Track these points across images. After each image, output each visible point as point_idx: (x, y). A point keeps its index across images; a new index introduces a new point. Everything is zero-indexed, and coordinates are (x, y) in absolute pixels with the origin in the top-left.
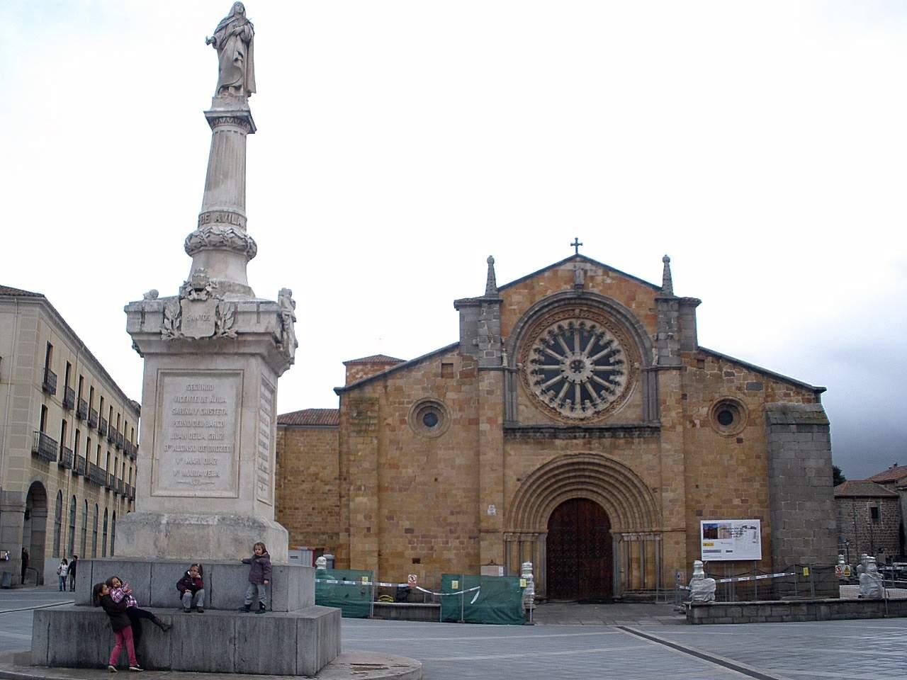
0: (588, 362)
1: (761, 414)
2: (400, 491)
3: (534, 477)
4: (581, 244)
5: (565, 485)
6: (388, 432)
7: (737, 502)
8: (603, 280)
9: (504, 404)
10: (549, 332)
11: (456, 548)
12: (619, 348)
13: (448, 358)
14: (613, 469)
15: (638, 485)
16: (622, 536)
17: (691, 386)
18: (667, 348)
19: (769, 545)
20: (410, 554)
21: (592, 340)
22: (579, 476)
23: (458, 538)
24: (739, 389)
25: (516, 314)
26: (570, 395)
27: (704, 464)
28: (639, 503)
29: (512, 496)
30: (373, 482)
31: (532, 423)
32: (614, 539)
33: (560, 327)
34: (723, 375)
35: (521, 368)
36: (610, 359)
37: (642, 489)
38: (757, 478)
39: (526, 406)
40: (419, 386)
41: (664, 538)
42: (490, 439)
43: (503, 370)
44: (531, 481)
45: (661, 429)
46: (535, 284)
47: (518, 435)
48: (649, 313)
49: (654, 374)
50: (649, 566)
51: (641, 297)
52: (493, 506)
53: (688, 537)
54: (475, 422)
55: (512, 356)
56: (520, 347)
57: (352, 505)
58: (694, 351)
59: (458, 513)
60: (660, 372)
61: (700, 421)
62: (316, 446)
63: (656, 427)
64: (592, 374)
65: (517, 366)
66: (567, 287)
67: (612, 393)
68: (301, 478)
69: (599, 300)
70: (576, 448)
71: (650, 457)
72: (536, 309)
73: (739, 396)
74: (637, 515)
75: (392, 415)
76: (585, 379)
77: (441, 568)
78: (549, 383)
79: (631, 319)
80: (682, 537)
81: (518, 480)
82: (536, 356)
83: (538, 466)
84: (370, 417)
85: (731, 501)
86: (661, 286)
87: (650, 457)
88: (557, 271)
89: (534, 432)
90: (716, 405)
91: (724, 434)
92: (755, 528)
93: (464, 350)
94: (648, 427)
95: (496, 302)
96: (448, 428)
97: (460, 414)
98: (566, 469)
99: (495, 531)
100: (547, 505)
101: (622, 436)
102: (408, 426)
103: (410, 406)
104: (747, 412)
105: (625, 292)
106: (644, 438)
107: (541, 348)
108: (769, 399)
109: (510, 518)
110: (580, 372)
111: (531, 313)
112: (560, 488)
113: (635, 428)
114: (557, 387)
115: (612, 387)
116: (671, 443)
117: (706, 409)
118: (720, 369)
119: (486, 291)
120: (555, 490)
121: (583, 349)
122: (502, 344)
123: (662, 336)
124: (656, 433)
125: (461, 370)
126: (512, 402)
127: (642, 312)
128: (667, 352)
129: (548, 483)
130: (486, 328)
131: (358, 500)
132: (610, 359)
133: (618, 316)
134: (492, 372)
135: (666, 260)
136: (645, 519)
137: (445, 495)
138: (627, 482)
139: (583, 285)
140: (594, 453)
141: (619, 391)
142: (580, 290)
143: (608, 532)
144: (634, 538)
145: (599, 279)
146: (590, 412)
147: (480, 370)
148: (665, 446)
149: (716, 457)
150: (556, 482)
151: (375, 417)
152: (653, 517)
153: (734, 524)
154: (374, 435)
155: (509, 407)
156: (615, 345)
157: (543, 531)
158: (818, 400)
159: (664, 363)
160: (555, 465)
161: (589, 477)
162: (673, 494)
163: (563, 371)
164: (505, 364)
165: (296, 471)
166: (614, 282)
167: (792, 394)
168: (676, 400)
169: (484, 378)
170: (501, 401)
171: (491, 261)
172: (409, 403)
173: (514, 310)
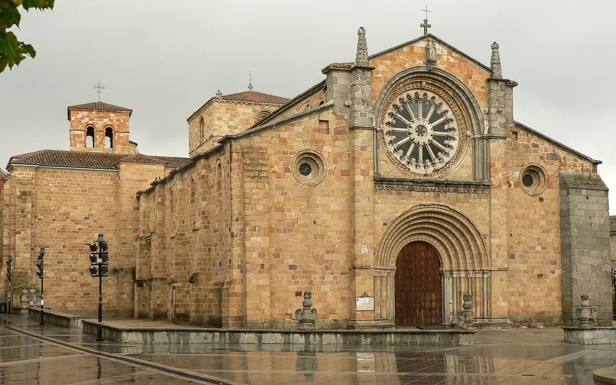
0: (429, 127)
4: (430, 27)
7: (538, 248)
10: (400, 99)
11: (330, 282)
12: (453, 117)
15: (473, 232)
23: (332, 273)
24: (542, 158)
26: (415, 154)
27: (517, 217)
29: (380, 238)
33: (408, 96)
34: (531, 146)
37: (475, 235)
39: (386, 162)
43: (373, 129)
49: (485, 141)
58: (510, 125)
59: (333, 252)
62: (66, 187)
66: (420, 62)
67: (447, 154)
68: (51, 217)
69: (445, 75)
71: (482, 209)
73: (542, 163)
75: (277, 164)
76: (427, 142)
77: (318, 300)
78: (399, 143)
81: (385, 224)
82: (390, 120)
85: (534, 248)
87: (482, 209)
97: (334, 165)
98: (418, 216)
103: (293, 156)
111: (393, 82)
115: (447, 150)
116: (498, 197)
117: (518, 173)
121: (425, 116)
123: (493, 110)
124: (486, 190)
130: (360, 91)
131: (254, 239)
133: (457, 91)
134: (365, 132)
135: (495, 47)
137: (322, 236)
138: (462, 229)
140: (441, 204)
141: (452, 153)
142: (432, 66)
145: (445, 58)
146: (430, 170)
148: (494, 201)
156: (450, 115)
158: (595, 171)
159: (494, 133)
165: (46, 210)
166: (456, 62)
169: (359, 135)
170: (372, 157)
171: (362, 33)
172: (292, 153)
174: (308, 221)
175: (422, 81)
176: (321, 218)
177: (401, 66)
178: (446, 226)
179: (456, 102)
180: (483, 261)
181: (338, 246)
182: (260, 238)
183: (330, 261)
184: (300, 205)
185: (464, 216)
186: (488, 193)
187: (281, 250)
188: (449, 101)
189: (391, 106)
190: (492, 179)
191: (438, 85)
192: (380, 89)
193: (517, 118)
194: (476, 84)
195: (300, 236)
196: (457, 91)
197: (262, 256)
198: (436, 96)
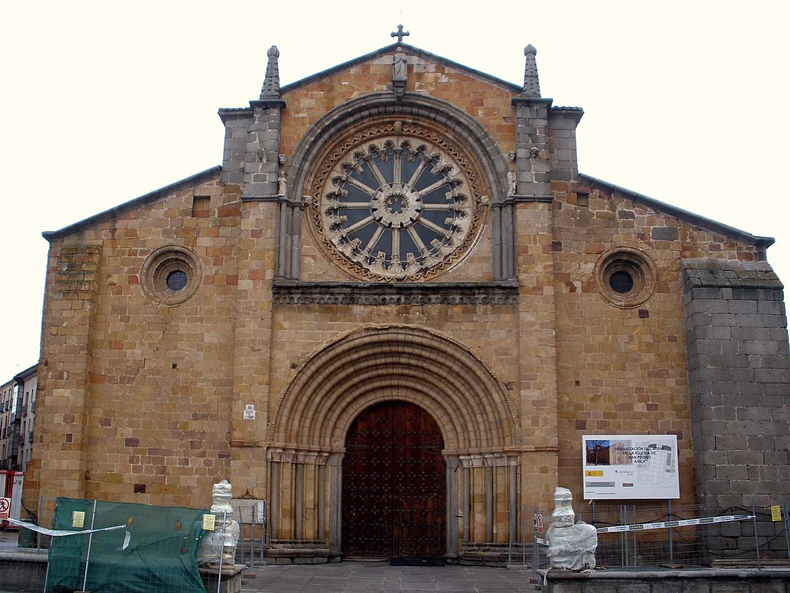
0: (412, 198)
1: (675, 274)
2: (122, 381)
3: (319, 363)
4: (408, 34)
5: (371, 379)
6: (111, 296)
8: (436, 79)
9: (278, 251)
10: (357, 155)
12: (461, 177)
13: (204, 189)
14: (445, 352)
15: (483, 377)
16: (460, 460)
17: (568, 230)
18: (530, 170)
19: (692, 475)
20: (132, 477)
21: (421, 167)
22: (393, 365)
23: (203, 455)
24: (642, 236)
27: (589, 349)
28: (484, 407)
29: (283, 391)
30: (79, 368)
31: (318, 280)
32: (448, 465)
33: (373, 149)
37: (489, 385)
38: (671, 371)
39: (314, 257)
40: (159, 229)
41: (523, 462)
42: (253, 303)
43: (279, 201)
44: (313, 368)
45: (520, 291)
46: (336, 84)
47: (296, 297)
48: (504, 123)
49: (509, 209)
50: (499, 506)
51: (490, 102)
52: (253, 406)
53: (561, 463)
54: (233, 280)
55: (296, 182)
56: (309, 173)
57: (48, 400)
58: (572, 181)
59: (205, 417)
60: (518, 206)
61: (582, 282)
63: (511, 288)
65: (303, 199)
66: (383, 88)
67: (449, 242)
69: (429, 105)
70: (386, 317)
71: (502, 333)
72: (335, 118)
73: (642, 247)
74: (482, 427)
75: (118, 271)
76: (406, 221)
79: (476, 131)
80: (552, 461)
81: (294, 366)
82: (335, 189)
83: (325, 345)
84: (85, 273)
85: (629, 407)
86: (522, 85)
87: (502, 333)
88: (369, 66)
90: (605, 261)
91: (619, 303)
92: (669, 448)
93: (227, 178)
94: (499, 287)
95: (274, 105)
96: (197, 289)
97: (214, 269)
98: (370, 351)
99: (253, 445)
100: (344, 410)
101: (457, 301)
102: (139, 286)
103: (145, 257)
104: (654, 272)
105: (469, 94)
106: (493, 305)
107: (344, 177)
108: (688, 253)
109: (277, 424)
110: (400, 212)
111: (327, 123)
112: (363, 382)
113: (479, 288)
114: (365, 234)
115: (448, 234)
116: (534, 312)
117: (591, 266)
118: (613, 208)
120: (355, 386)
121: (405, 180)
122: (280, 165)
123: (522, 153)
125: (221, 204)
127: (493, 122)
128: (529, 176)
129: (342, 375)
130: (257, 141)
134: (262, 206)
135: (530, 52)
136: (494, 432)
137: (186, 390)
139: (405, 82)
141: (458, 239)
142: (401, 90)
143: (440, 452)
144: (477, 463)
145: (430, 77)
146: (413, 270)
147: (246, 200)
148: (526, 317)
149: (607, 339)
150: (356, 373)
151: (90, 273)
152: (506, 429)
153: (637, 441)
154: (87, 296)
155: (283, 256)
156: (454, 174)
157: (335, 450)
159: (525, 193)
160: (352, 344)
161: (409, 366)
162: (537, 392)
163: (375, 210)
164: (283, 192)
166: (452, 81)
167: (722, 246)
168: (544, 248)
171: (274, 54)
172: (143, 253)
174: (163, 364)
175: (394, 120)
176: (187, 358)
177: (343, 97)
178: (435, 369)
180: (507, 433)
181: (216, 408)
182: (69, 390)
183: (198, 432)
184: (150, 336)
185: (461, 348)
187: (114, 412)
188: (451, 150)
189: (338, 167)
190: (522, 276)
191: (425, 124)
193: (586, 167)
194: (491, 115)
195: (147, 389)
197: (70, 421)
198: (427, 144)
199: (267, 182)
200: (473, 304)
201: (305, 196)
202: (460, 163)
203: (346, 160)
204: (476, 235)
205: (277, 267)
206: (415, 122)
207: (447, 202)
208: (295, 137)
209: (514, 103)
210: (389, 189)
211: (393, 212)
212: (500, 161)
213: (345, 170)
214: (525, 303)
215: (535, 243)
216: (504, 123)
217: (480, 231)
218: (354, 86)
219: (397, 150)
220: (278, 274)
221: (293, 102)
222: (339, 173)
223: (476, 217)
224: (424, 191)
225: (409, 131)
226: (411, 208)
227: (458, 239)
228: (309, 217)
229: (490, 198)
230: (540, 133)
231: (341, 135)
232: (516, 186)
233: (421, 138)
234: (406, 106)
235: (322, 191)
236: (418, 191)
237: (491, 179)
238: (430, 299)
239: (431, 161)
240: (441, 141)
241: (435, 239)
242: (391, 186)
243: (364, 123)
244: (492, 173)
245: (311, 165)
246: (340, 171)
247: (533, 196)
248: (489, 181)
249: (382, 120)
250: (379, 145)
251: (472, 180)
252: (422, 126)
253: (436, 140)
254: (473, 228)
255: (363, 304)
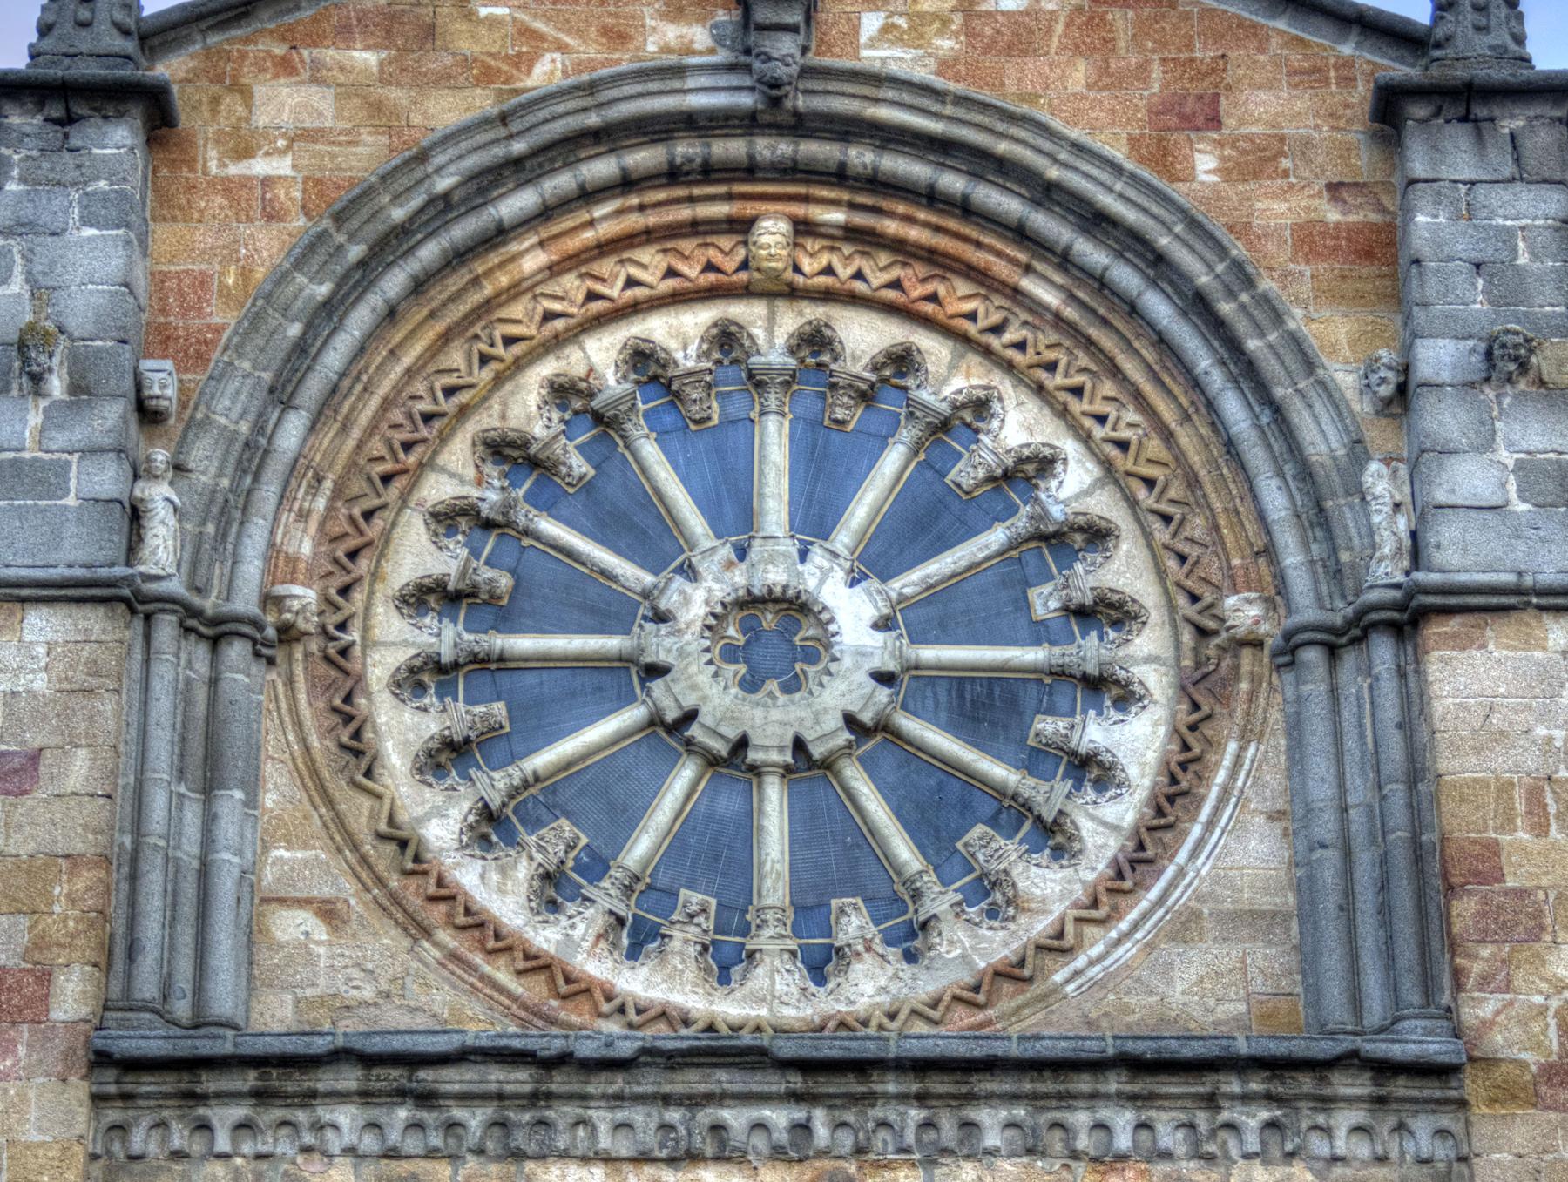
0: (852, 612)
9: (127, 866)
10: (561, 392)
12: (1105, 506)
18: (1486, 445)
25: (272, 215)
31: (348, 1029)
33: (642, 359)
35: (309, 624)
36: (1034, 594)
39: (329, 912)
45: (1472, 1085)
48: (1333, 216)
49: (1383, 650)
60: (1434, 630)
64: (883, 694)
65: (270, 600)
72: (443, 184)
89: (365, 1096)
94: (1351, 1060)
95: (111, 96)
105: (1143, 69)
107: (490, 498)
110: (792, 686)
111: (398, 214)
115: (1049, 794)
119: (45, 30)
121: (814, 521)
123: (1439, 357)
126: (205, 872)
127: (1277, 209)
132: (1034, 594)
133: (1092, 253)
141: (1105, 824)
142: (786, 45)
156: (1075, 486)
159: (1461, 555)
163: (655, 671)
173: (267, 182)
175: (750, 209)
177: (487, 76)
179: (1115, 372)
186: (1443, 1151)
189: (459, 453)
191: (914, 234)
192: (260, 273)
196: (1092, 253)
199: (71, 501)
200: (1210, 1158)
201: (280, 590)
202: (1099, 432)
203: (503, 417)
204: (1201, 800)
205: (119, 952)
206: (861, 219)
207: (1039, 633)
208: (230, 281)
209: (1389, 108)
210: (729, 565)
211: (751, 684)
212: (1319, 407)
213: (491, 470)
214: (1505, 1157)
215: (1541, 829)
216: (1333, 216)
217: (1221, 777)
218: (539, 25)
219: (769, 369)
220: (127, 990)
221: (215, 100)
222: (462, 481)
223: (1196, 706)
224: (915, 575)
225: (829, 270)
226: (847, 662)
227: (1104, 824)
228: (302, 697)
229: (1269, 602)
230: (1534, 255)
231: (476, 282)
232: (1414, 535)
233: (890, 309)
234: (811, 134)
235: (376, 575)
236: (884, 578)
237: (1275, 500)
238: (968, 1126)
239: (944, 426)
240: (996, 318)
241: (979, 829)
242: (742, 553)
243: (591, 223)
244: (1280, 473)
245: (312, 428)
246: (471, 473)
247: (1507, 578)
248: (1261, 517)
249: (684, 213)
250: (673, 345)
251: (1167, 519)
252: (898, 246)
253: (972, 317)
254: (1183, 766)
255: (608, 1159)
